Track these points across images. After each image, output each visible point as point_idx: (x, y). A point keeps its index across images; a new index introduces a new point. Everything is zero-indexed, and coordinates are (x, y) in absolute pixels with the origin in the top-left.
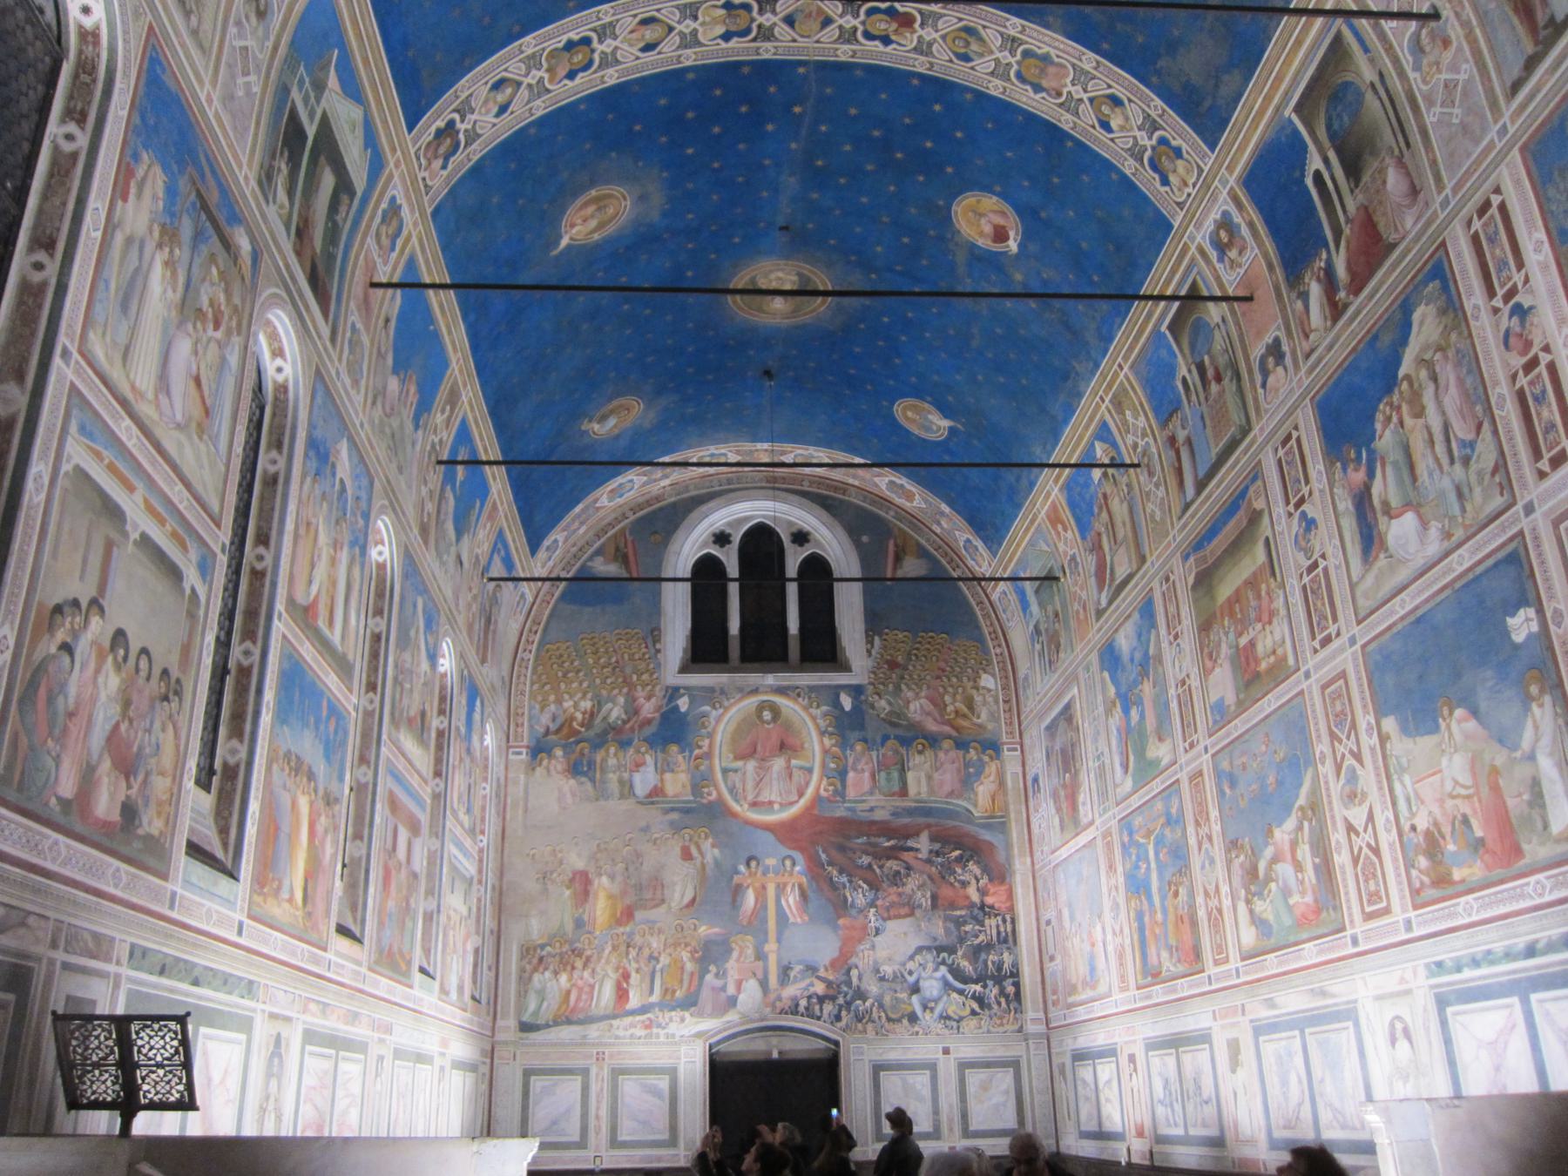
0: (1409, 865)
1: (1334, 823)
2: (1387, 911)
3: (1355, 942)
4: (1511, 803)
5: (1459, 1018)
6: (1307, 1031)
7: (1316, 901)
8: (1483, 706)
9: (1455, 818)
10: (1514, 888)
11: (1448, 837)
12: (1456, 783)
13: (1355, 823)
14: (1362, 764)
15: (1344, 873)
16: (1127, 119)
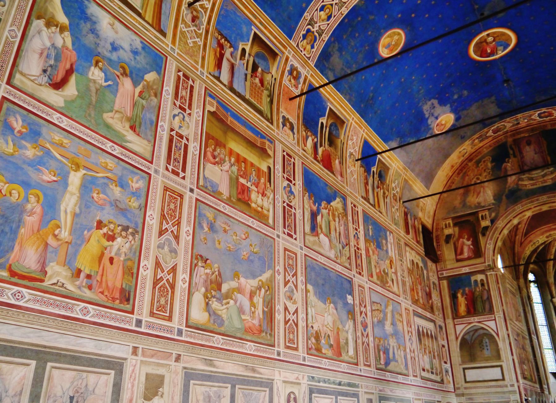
0: (308, 339)
1: (279, 301)
2: (296, 349)
3: (279, 354)
4: (341, 340)
5: (316, 398)
6: (237, 386)
7: (260, 325)
8: (338, 309)
9: (326, 334)
10: (339, 364)
11: (323, 338)
12: (328, 324)
13: (290, 309)
14: (297, 291)
15: (279, 323)
16: (323, 21)
